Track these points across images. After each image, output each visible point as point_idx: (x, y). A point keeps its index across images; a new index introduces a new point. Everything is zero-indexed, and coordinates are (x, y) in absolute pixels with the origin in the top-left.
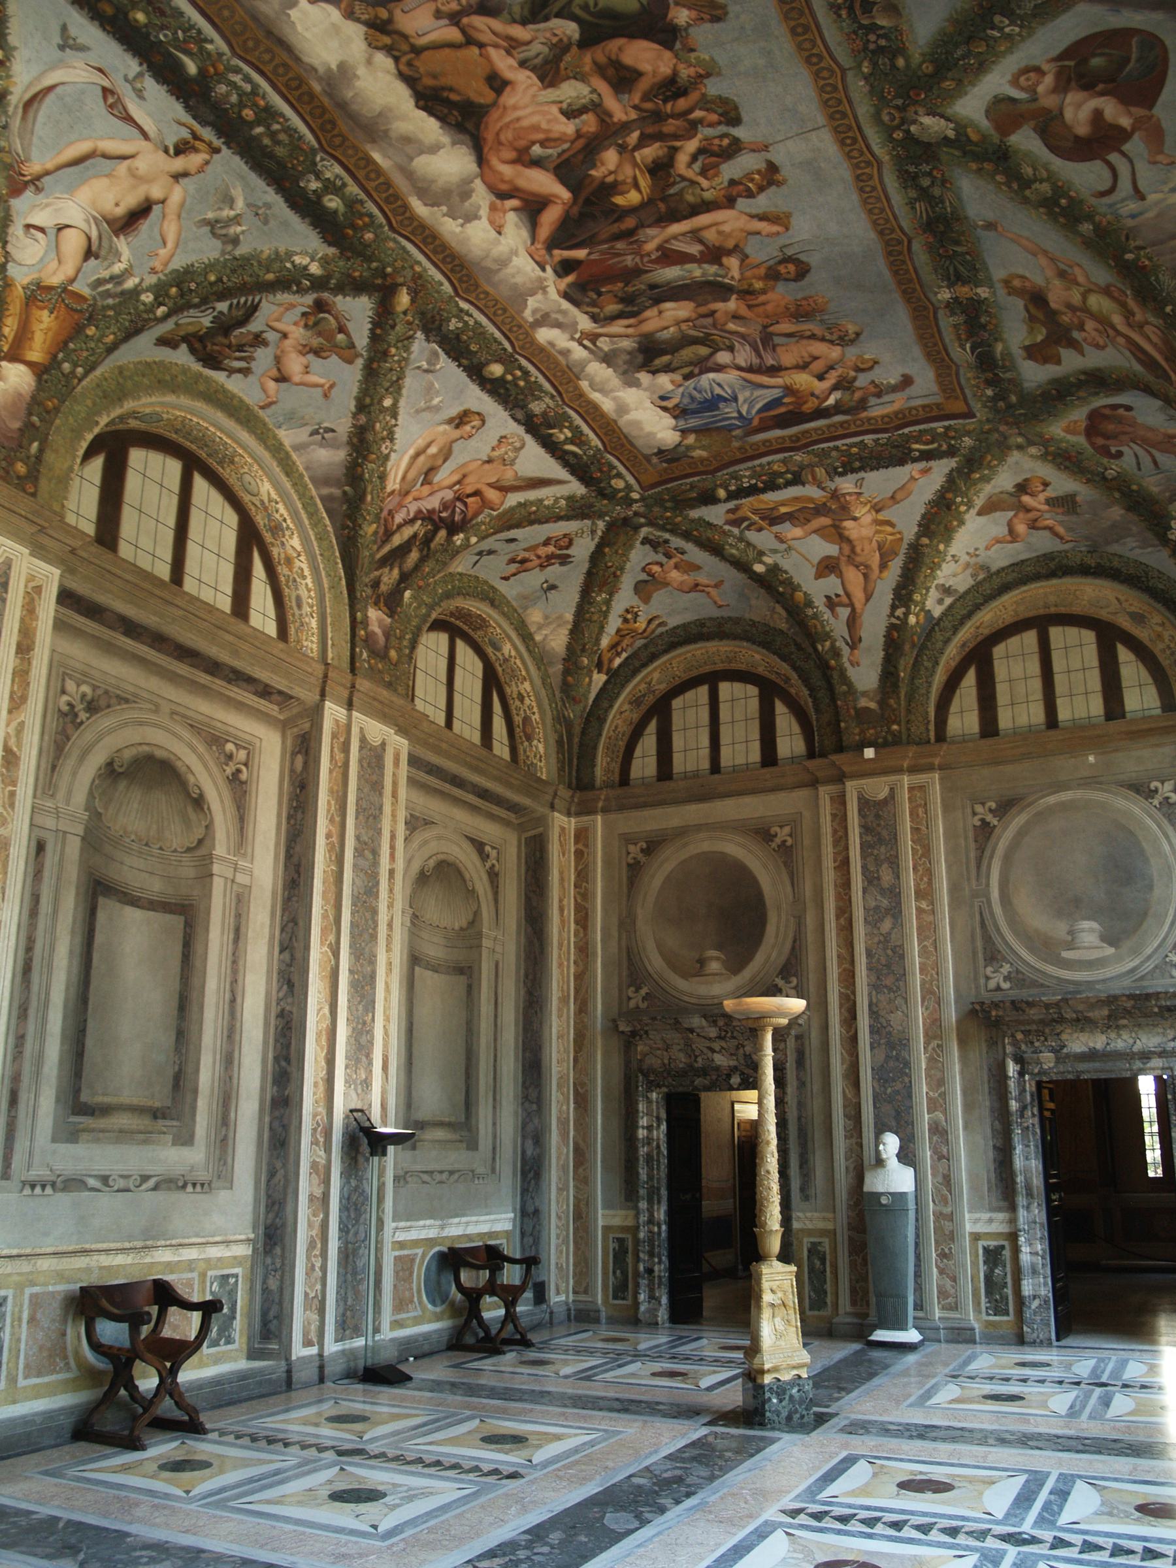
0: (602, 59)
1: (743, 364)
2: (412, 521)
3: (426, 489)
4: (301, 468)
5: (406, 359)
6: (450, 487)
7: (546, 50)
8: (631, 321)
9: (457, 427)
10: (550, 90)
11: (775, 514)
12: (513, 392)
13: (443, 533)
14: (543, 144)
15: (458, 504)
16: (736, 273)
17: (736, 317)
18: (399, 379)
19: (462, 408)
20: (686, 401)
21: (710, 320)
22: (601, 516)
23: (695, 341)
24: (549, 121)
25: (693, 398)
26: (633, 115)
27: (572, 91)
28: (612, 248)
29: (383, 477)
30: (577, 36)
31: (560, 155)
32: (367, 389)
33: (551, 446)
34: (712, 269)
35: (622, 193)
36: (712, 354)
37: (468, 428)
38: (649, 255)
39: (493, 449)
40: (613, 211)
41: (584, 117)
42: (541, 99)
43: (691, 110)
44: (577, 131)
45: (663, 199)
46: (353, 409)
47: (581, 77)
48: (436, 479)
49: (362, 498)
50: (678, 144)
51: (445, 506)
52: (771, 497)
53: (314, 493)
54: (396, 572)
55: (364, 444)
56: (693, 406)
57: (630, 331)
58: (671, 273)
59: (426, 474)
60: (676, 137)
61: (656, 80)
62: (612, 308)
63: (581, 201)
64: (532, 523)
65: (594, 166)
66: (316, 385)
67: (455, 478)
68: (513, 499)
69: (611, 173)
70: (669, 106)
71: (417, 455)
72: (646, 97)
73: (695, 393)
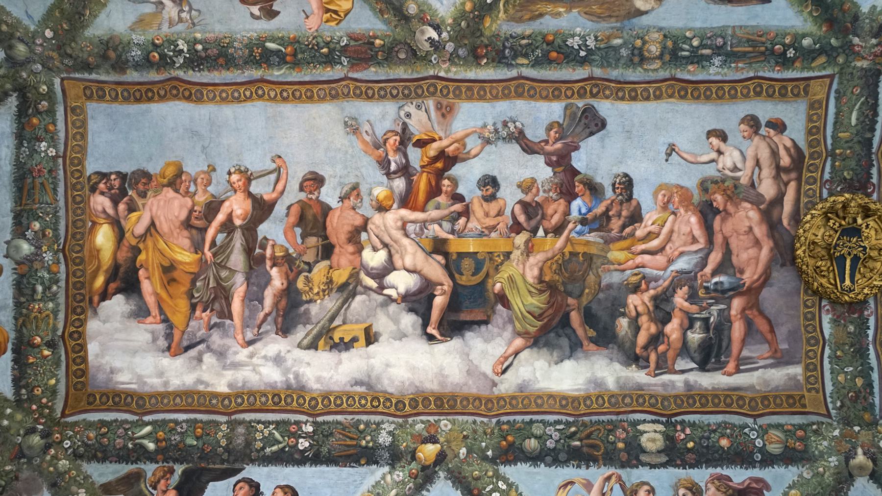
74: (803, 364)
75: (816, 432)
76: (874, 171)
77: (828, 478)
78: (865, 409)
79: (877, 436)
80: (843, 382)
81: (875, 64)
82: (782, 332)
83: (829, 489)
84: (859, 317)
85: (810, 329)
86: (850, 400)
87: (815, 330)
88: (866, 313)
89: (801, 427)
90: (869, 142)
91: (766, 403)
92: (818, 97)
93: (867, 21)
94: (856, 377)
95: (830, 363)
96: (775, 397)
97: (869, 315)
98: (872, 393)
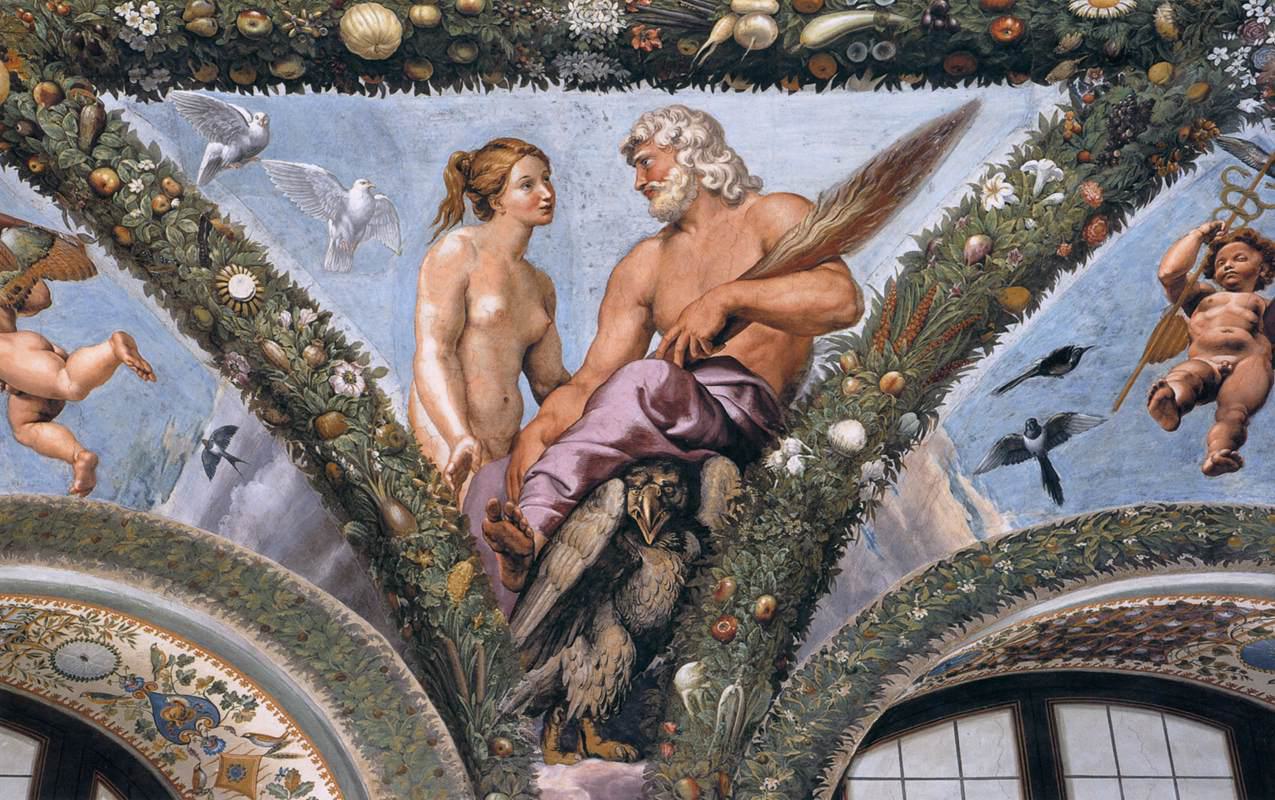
2: (590, 493)
3: (565, 404)
4: (251, 553)
5: (163, 170)
6: (639, 350)
9: (486, 211)
12: (489, 35)
13: (719, 474)
15: (702, 377)
18: (205, 222)
19: (440, 167)
22: (1223, 112)
29: (402, 447)
32: (176, 295)
33: (772, 67)
37: (515, 195)
39: (649, 193)
46: (205, 356)
48: (572, 361)
49: (381, 526)
51: (667, 406)
53: (305, 584)
54: (614, 643)
55: (301, 403)
59: (527, 365)
64: (1037, 277)
66: (111, 366)
67: (627, 325)
68: (879, 262)
71: (454, 344)
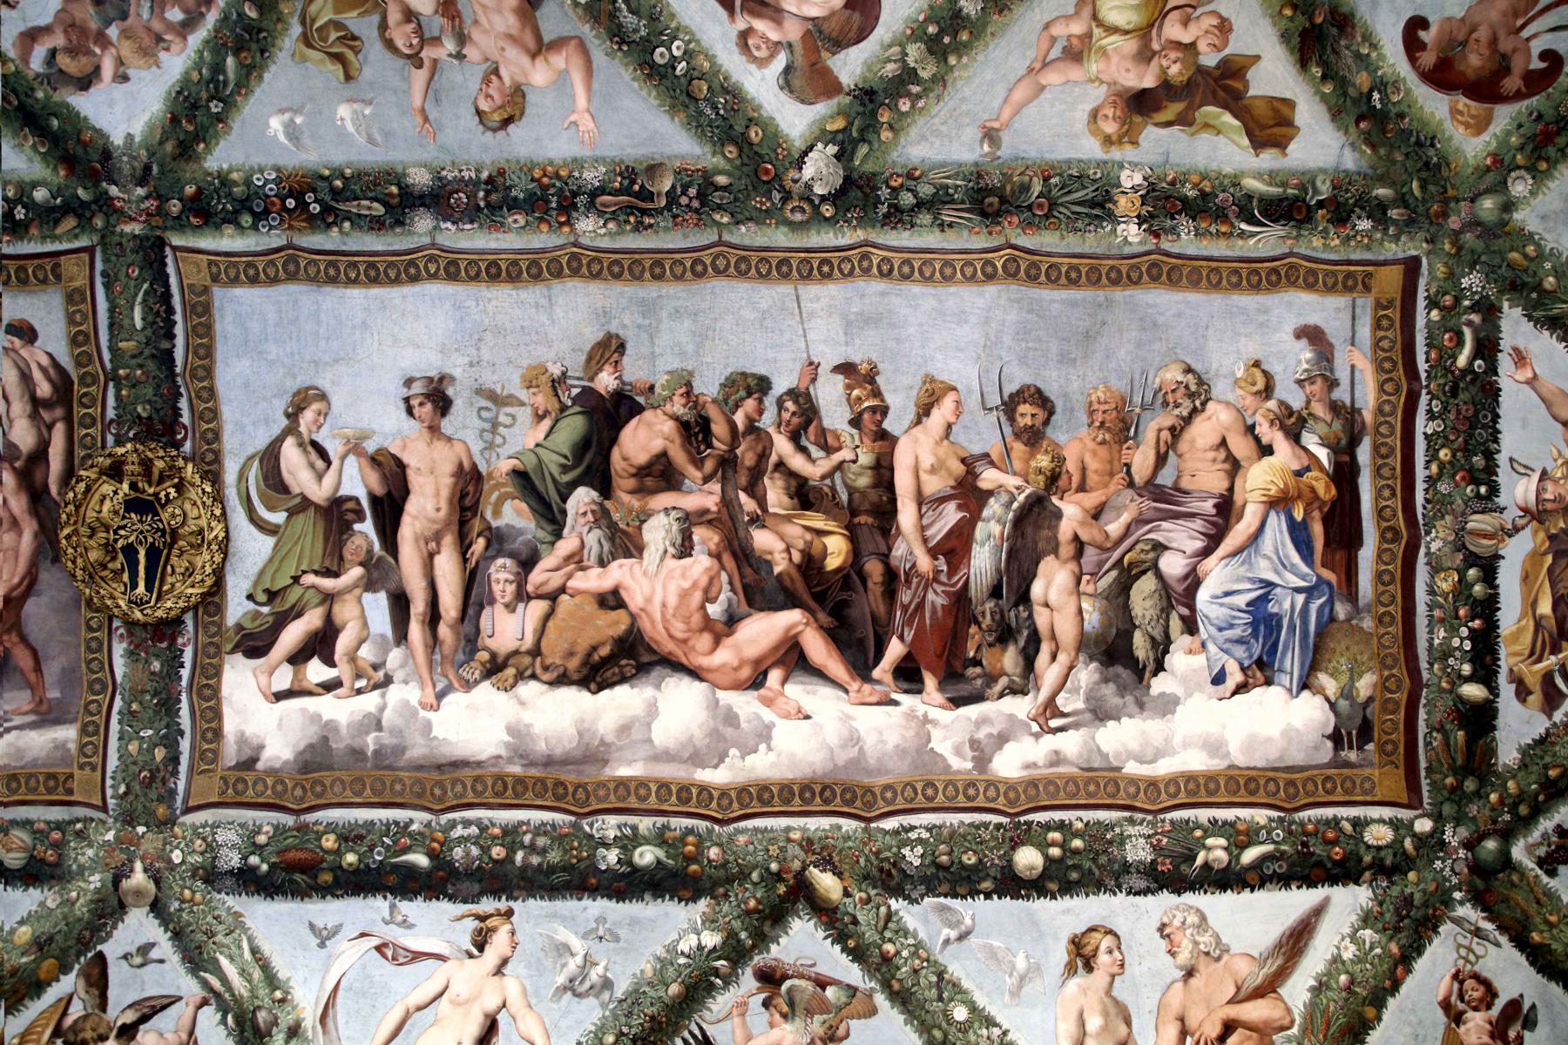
0: (631, 483)
1: (1199, 544)
7: (597, 533)
8: (1045, 649)
10: (646, 554)
11: (1551, 624)
14: (709, 598)
16: (1012, 482)
17: (1097, 514)
20: (1240, 651)
21: (1090, 555)
23: (1123, 588)
24: (683, 576)
25: (1240, 641)
26: (716, 487)
27: (658, 532)
28: (905, 608)
30: (594, 494)
31: (733, 590)
34: (994, 507)
35: (824, 554)
36: (1159, 576)
38: (937, 572)
40: (847, 577)
41: (695, 538)
42: (652, 568)
43: (732, 426)
44: (710, 554)
45: (854, 512)
47: (644, 516)
50: (773, 459)
52: (1510, 615)
56: (1257, 649)
57: (1063, 658)
58: (983, 561)
60: (763, 456)
61: (678, 441)
62: (1010, 659)
63: (812, 603)
65: (769, 565)
69: (788, 550)
70: (716, 443)
72: (698, 463)
73: (1229, 633)
74: (78, 725)
75: (79, 835)
76: (183, 404)
77: (81, 909)
78: (160, 799)
79: (170, 843)
80: (135, 753)
81: (153, 228)
82: (52, 670)
83: (78, 927)
84: (169, 648)
85: (94, 665)
86: (142, 783)
87: (102, 669)
88: (180, 641)
89: (59, 826)
90: (167, 358)
91: (14, 785)
92: (77, 284)
93: (125, 159)
94: (156, 745)
95: (120, 722)
96: (31, 776)
97: (184, 645)
98: (175, 773)
